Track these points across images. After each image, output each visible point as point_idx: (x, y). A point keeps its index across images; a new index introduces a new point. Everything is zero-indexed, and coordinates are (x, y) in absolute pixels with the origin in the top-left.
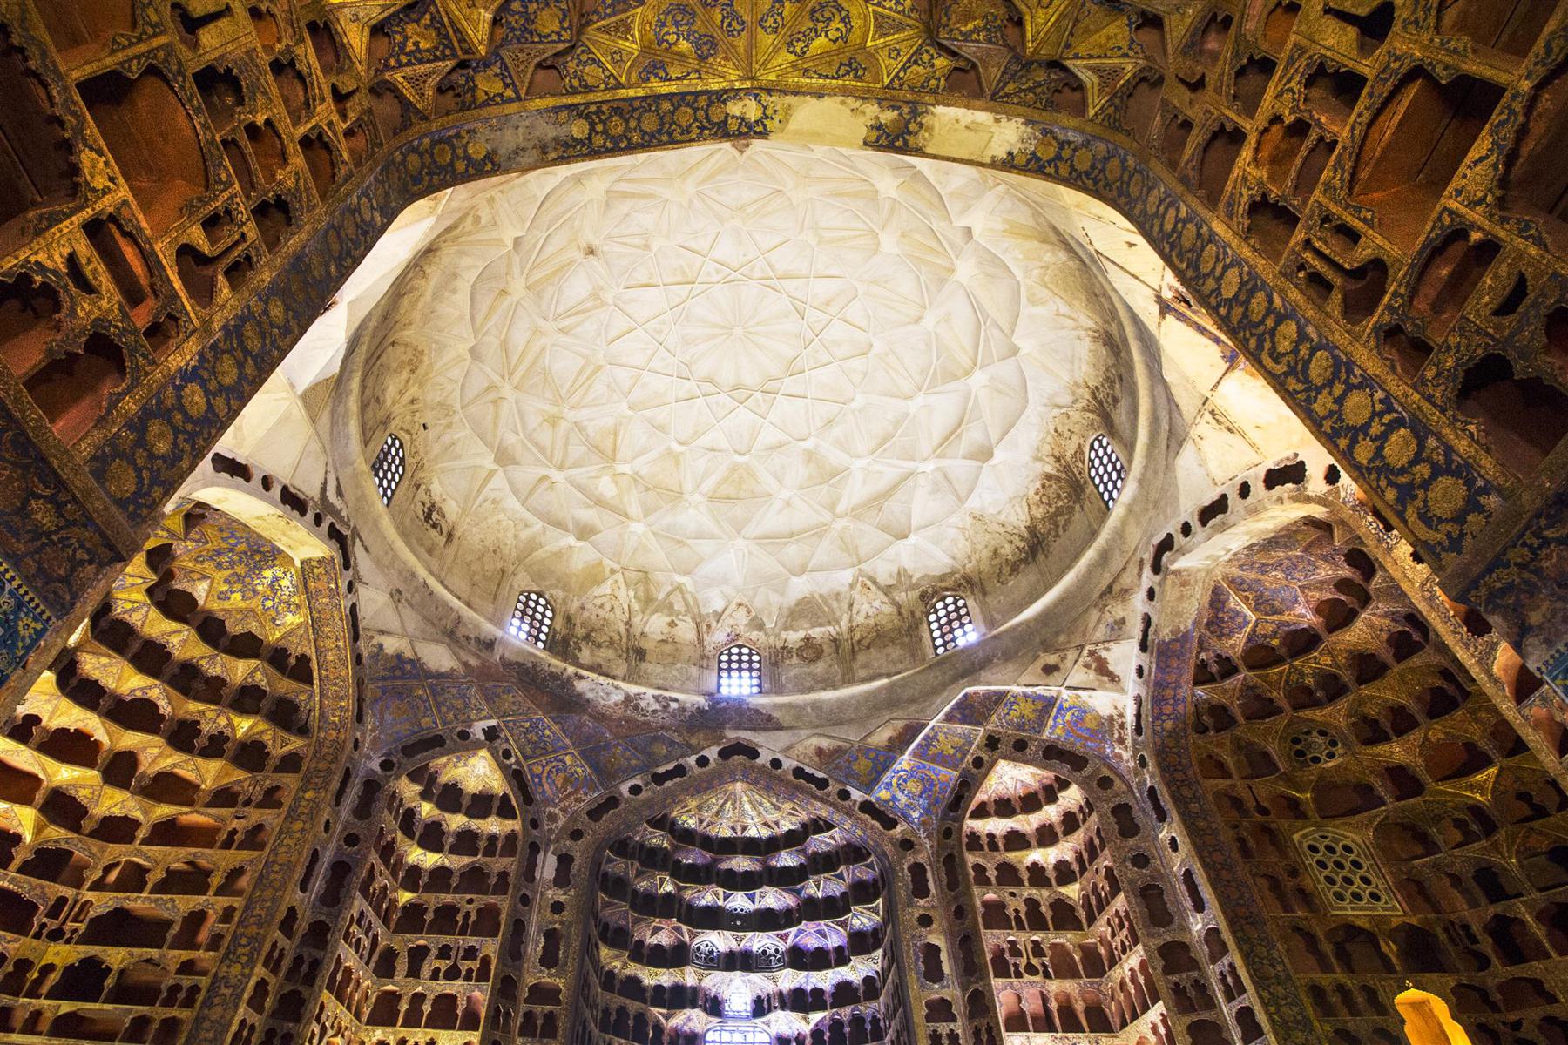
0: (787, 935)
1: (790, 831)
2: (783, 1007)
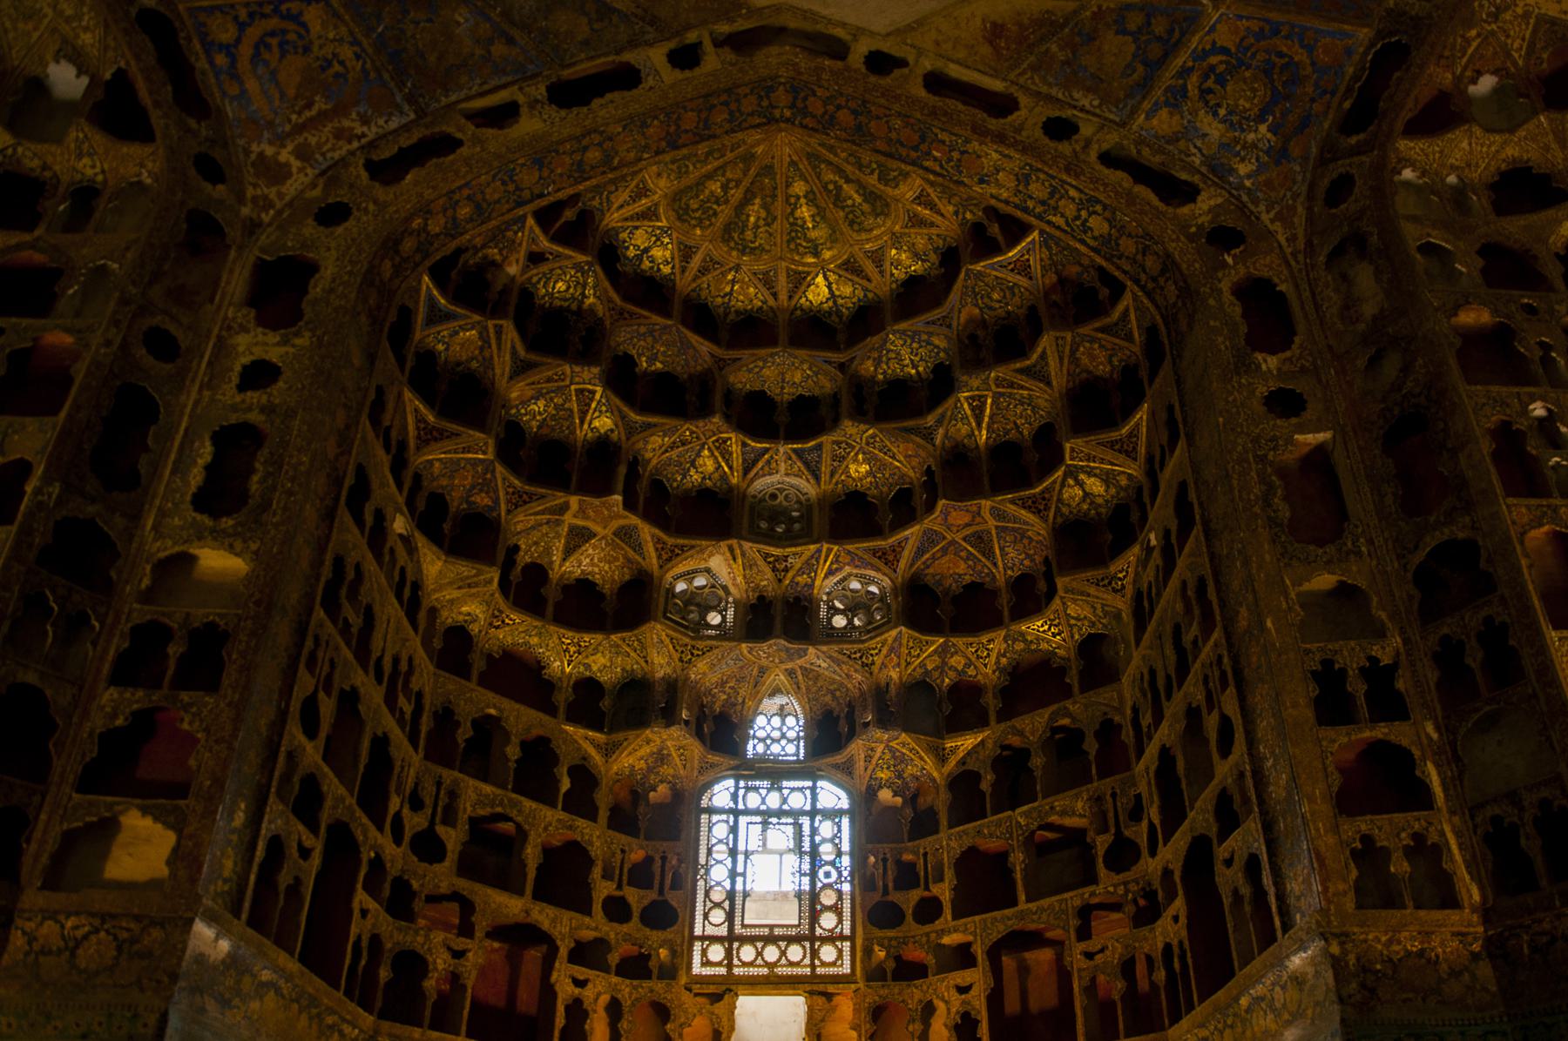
0: (896, 550)
1: (913, 282)
2: (884, 721)
